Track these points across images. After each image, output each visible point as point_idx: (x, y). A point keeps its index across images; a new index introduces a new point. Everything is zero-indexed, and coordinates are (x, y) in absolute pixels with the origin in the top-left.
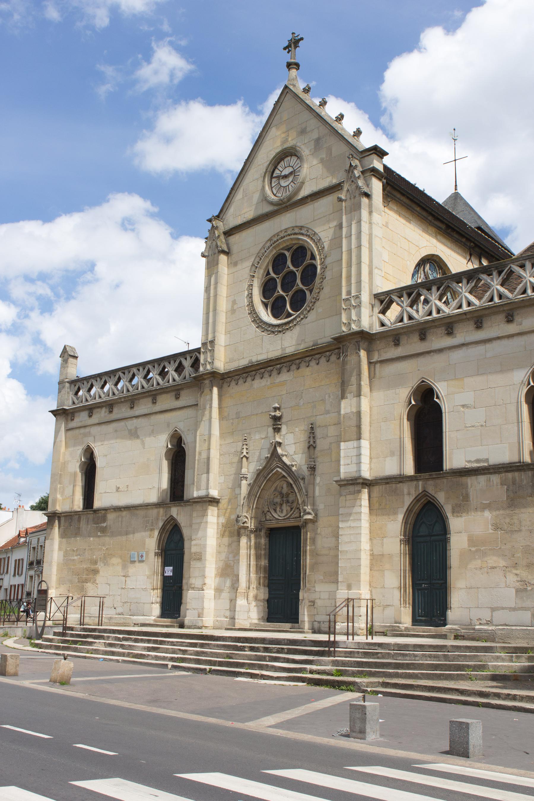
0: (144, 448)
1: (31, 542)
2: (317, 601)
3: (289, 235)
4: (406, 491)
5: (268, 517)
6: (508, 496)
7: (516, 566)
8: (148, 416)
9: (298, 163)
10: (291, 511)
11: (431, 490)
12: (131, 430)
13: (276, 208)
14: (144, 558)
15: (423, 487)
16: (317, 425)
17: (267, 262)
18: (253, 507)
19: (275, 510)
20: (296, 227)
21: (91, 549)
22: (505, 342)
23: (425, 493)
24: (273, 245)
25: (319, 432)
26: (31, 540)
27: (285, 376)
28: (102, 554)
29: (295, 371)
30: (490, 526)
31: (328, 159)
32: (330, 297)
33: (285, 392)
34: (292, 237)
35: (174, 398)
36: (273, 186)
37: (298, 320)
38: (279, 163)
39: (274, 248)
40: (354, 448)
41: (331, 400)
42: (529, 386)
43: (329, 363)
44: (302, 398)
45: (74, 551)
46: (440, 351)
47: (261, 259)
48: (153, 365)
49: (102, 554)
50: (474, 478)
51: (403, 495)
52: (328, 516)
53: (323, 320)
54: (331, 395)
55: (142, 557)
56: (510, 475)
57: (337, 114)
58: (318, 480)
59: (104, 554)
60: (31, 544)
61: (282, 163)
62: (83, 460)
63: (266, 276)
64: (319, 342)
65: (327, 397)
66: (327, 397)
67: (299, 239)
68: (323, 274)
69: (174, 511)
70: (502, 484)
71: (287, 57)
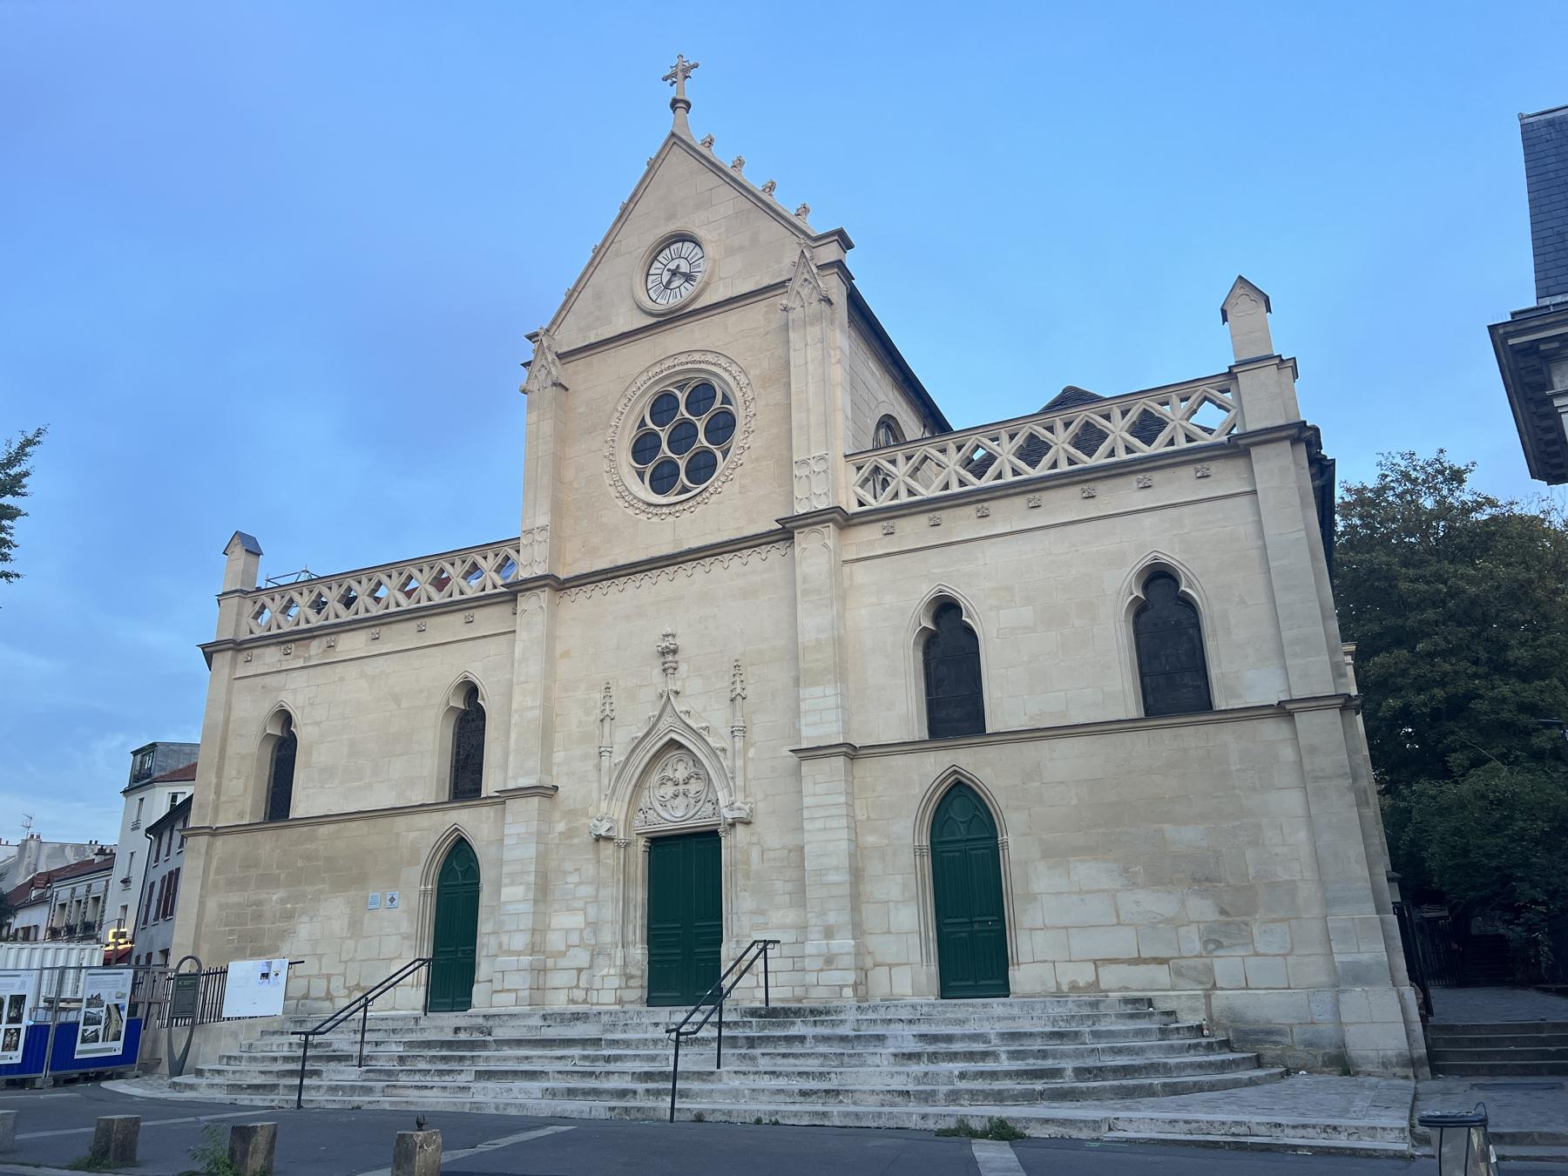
1: (57, 895)
9: (697, 254)
13: (655, 320)
26: (58, 892)
36: (649, 287)
37: (704, 496)
39: (656, 383)
40: (825, 696)
42: (1133, 597)
47: (630, 400)
55: (392, 902)
57: (766, 181)
60: (56, 899)
63: (638, 428)
68: (748, 425)
71: (672, 93)
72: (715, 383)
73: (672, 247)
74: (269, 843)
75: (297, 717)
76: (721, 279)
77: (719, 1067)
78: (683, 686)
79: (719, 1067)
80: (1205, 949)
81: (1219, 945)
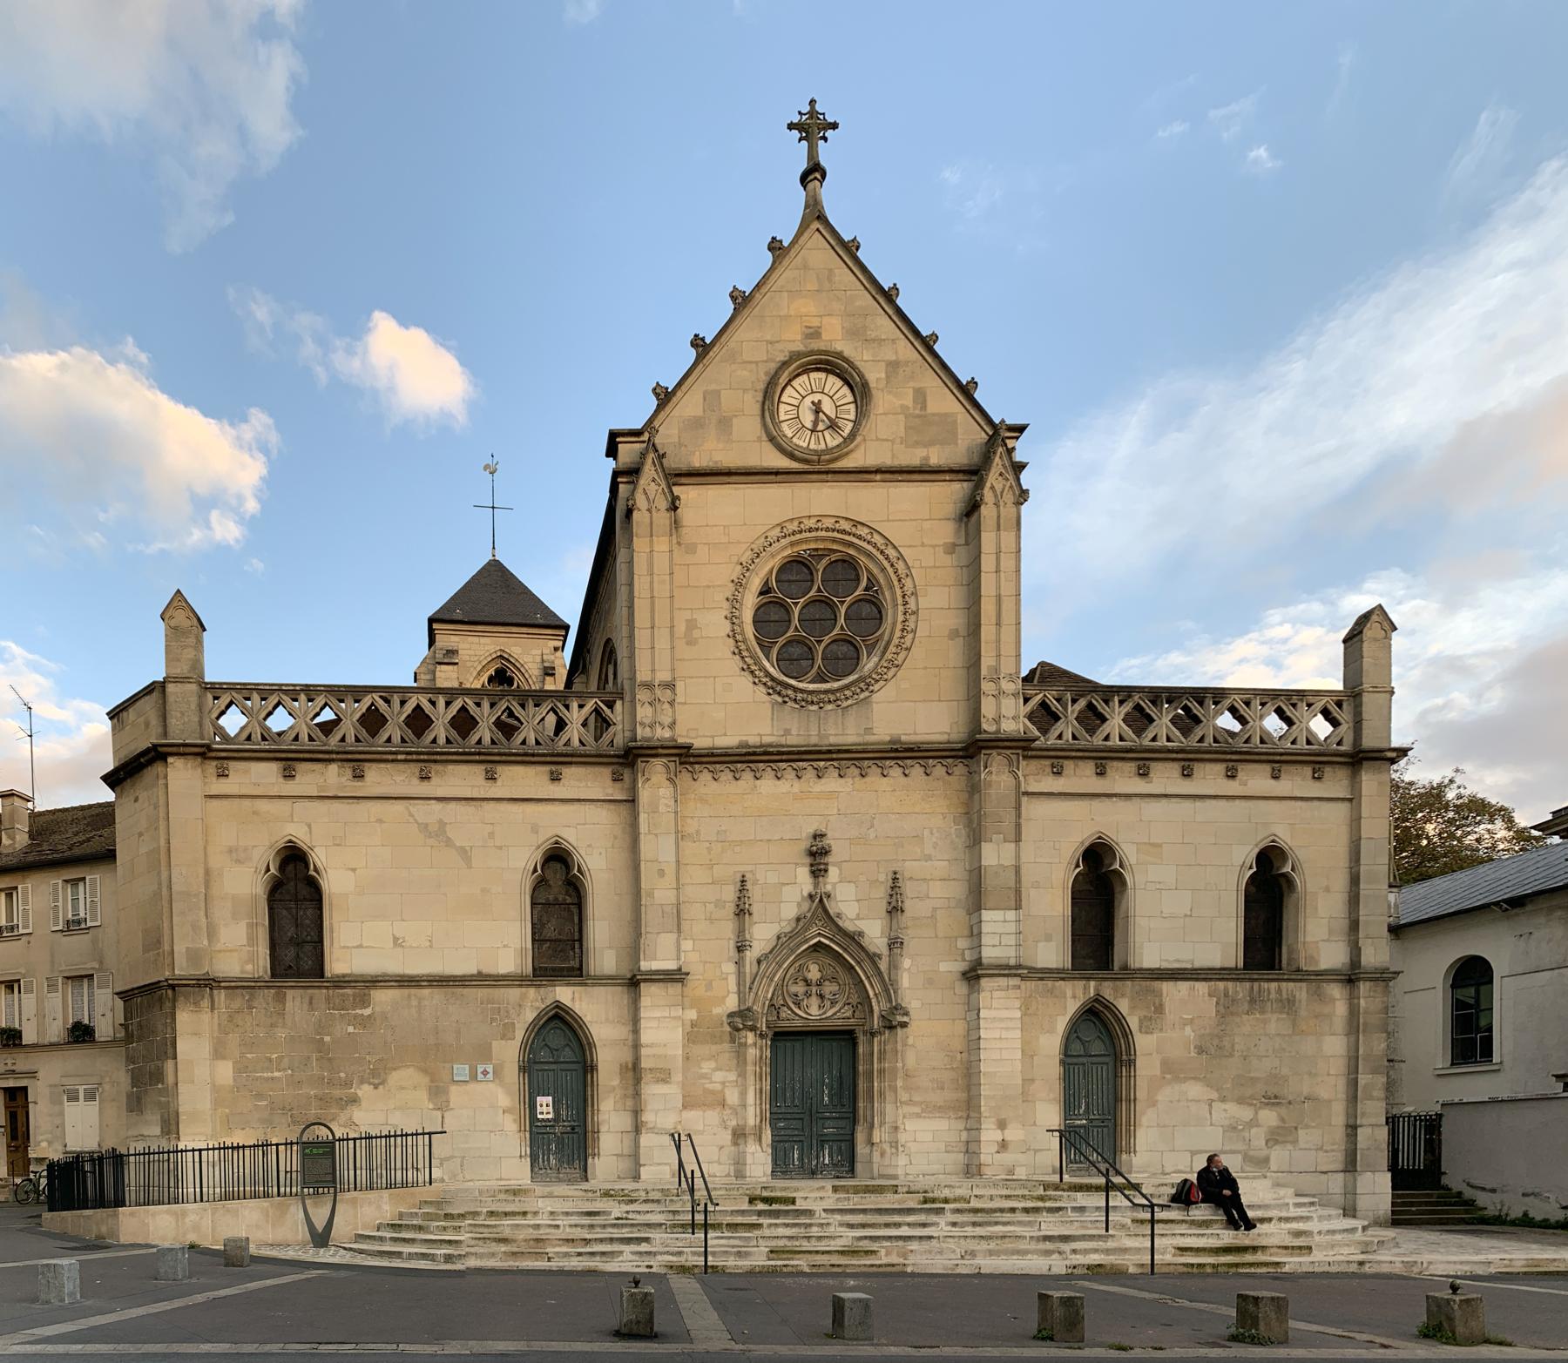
0: (469, 866)
2: (908, 1145)
3: (827, 530)
4: (1069, 993)
5: (783, 1015)
6: (1217, 1011)
7: (1223, 1099)
8: (479, 803)
10: (831, 1008)
11: (1108, 991)
12: (427, 825)
13: (794, 465)
14: (490, 1076)
15: (1096, 989)
16: (907, 875)
17: (769, 565)
18: (765, 998)
19: (798, 1005)
20: (847, 519)
21: (330, 1060)
22: (1222, 803)
23: (1098, 999)
24: (788, 540)
25: (909, 889)
27: (831, 783)
28: (364, 1071)
29: (856, 779)
30: (1192, 1047)
31: (917, 412)
32: (925, 668)
33: (835, 811)
34: (836, 534)
35: (546, 777)
38: (798, 375)
39: (792, 544)
41: (934, 840)
43: (930, 777)
44: (872, 826)
45: (270, 1060)
46: (1128, 796)
48: (477, 701)
49: (364, 1071)
50: (1171, 984)
51: (1065, 997)
52: (930, 1019)
53: (912, 704)
54: (935, 831)
55: (485, 1075)
56: (1221, 985)
58: (906, 963)
59: (371, 1070)
61: (805, 377)
62: (273, 870)
64: (903, 738)
65: (926, 833)
66: (926, 833)
67: (851, 544)
69: (565, 994)
70: (1210, 995)
72: (863, 560)
73: (814, 375)
74: (296, 1000)
75: (320, 857)
76: (877, 439)
77: (1107, 1230)
78: (834, 888)
79: (1107, 1230)
80: (1266, 1144)
81: (1277, 1142)
